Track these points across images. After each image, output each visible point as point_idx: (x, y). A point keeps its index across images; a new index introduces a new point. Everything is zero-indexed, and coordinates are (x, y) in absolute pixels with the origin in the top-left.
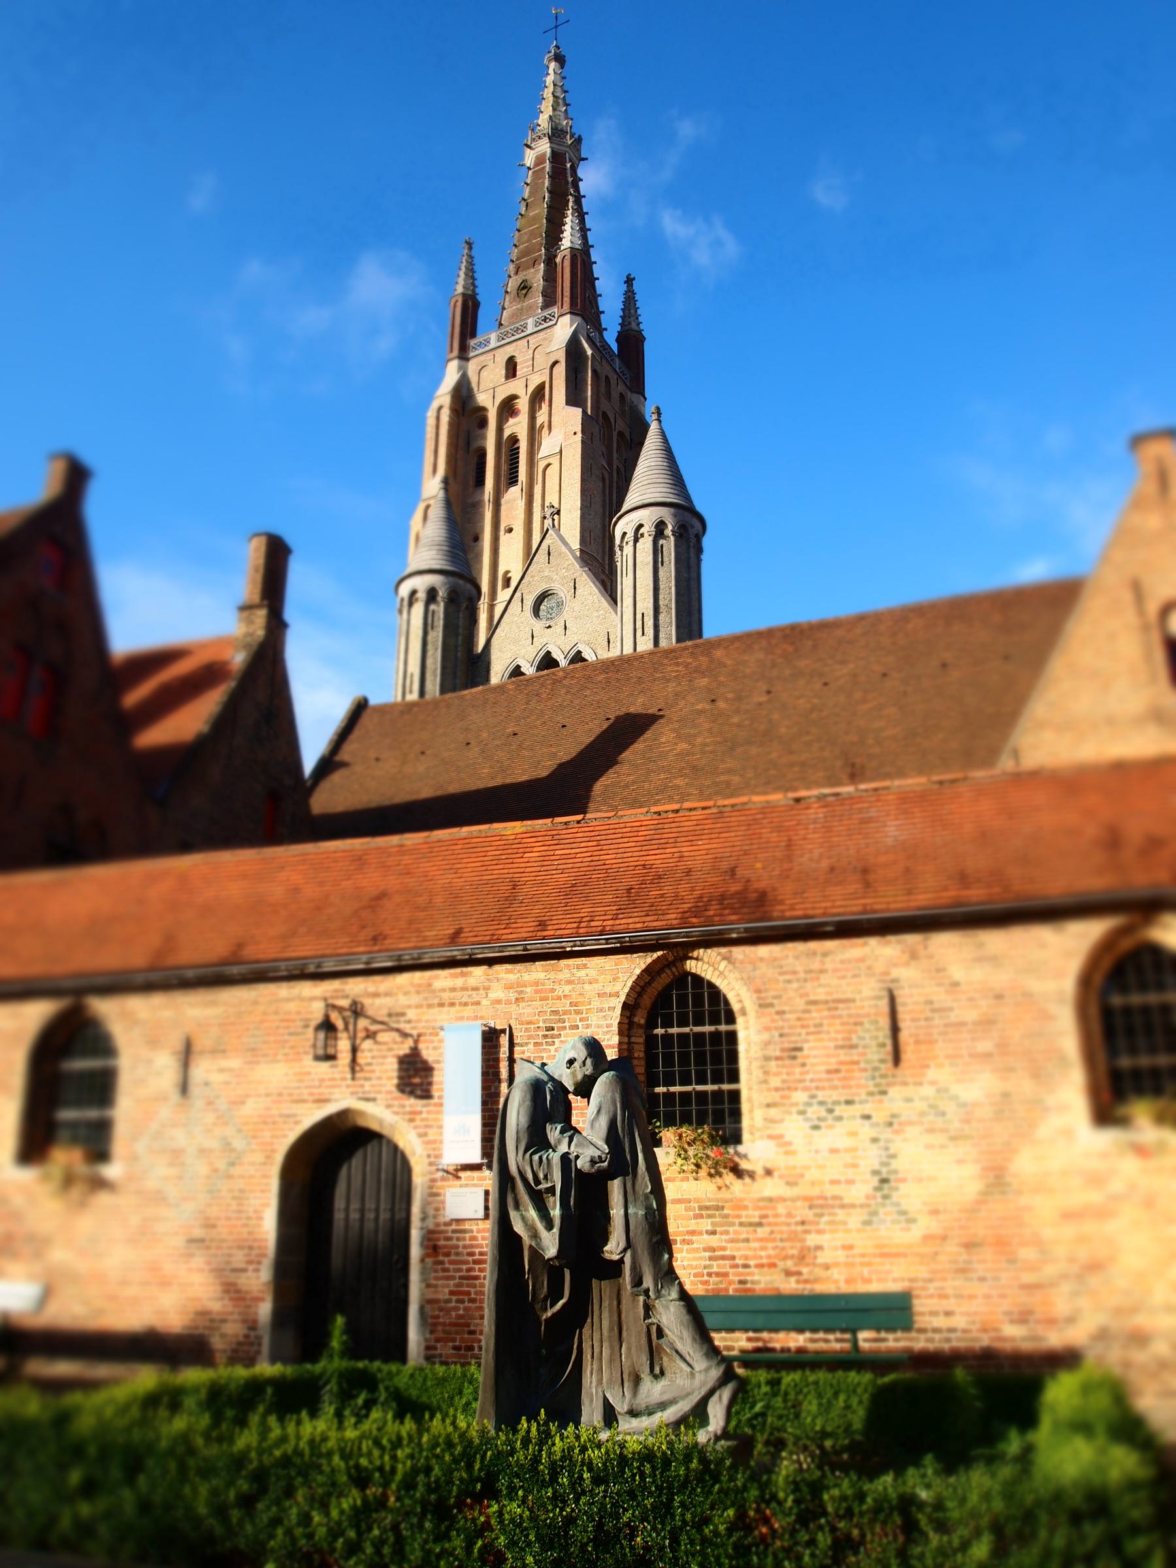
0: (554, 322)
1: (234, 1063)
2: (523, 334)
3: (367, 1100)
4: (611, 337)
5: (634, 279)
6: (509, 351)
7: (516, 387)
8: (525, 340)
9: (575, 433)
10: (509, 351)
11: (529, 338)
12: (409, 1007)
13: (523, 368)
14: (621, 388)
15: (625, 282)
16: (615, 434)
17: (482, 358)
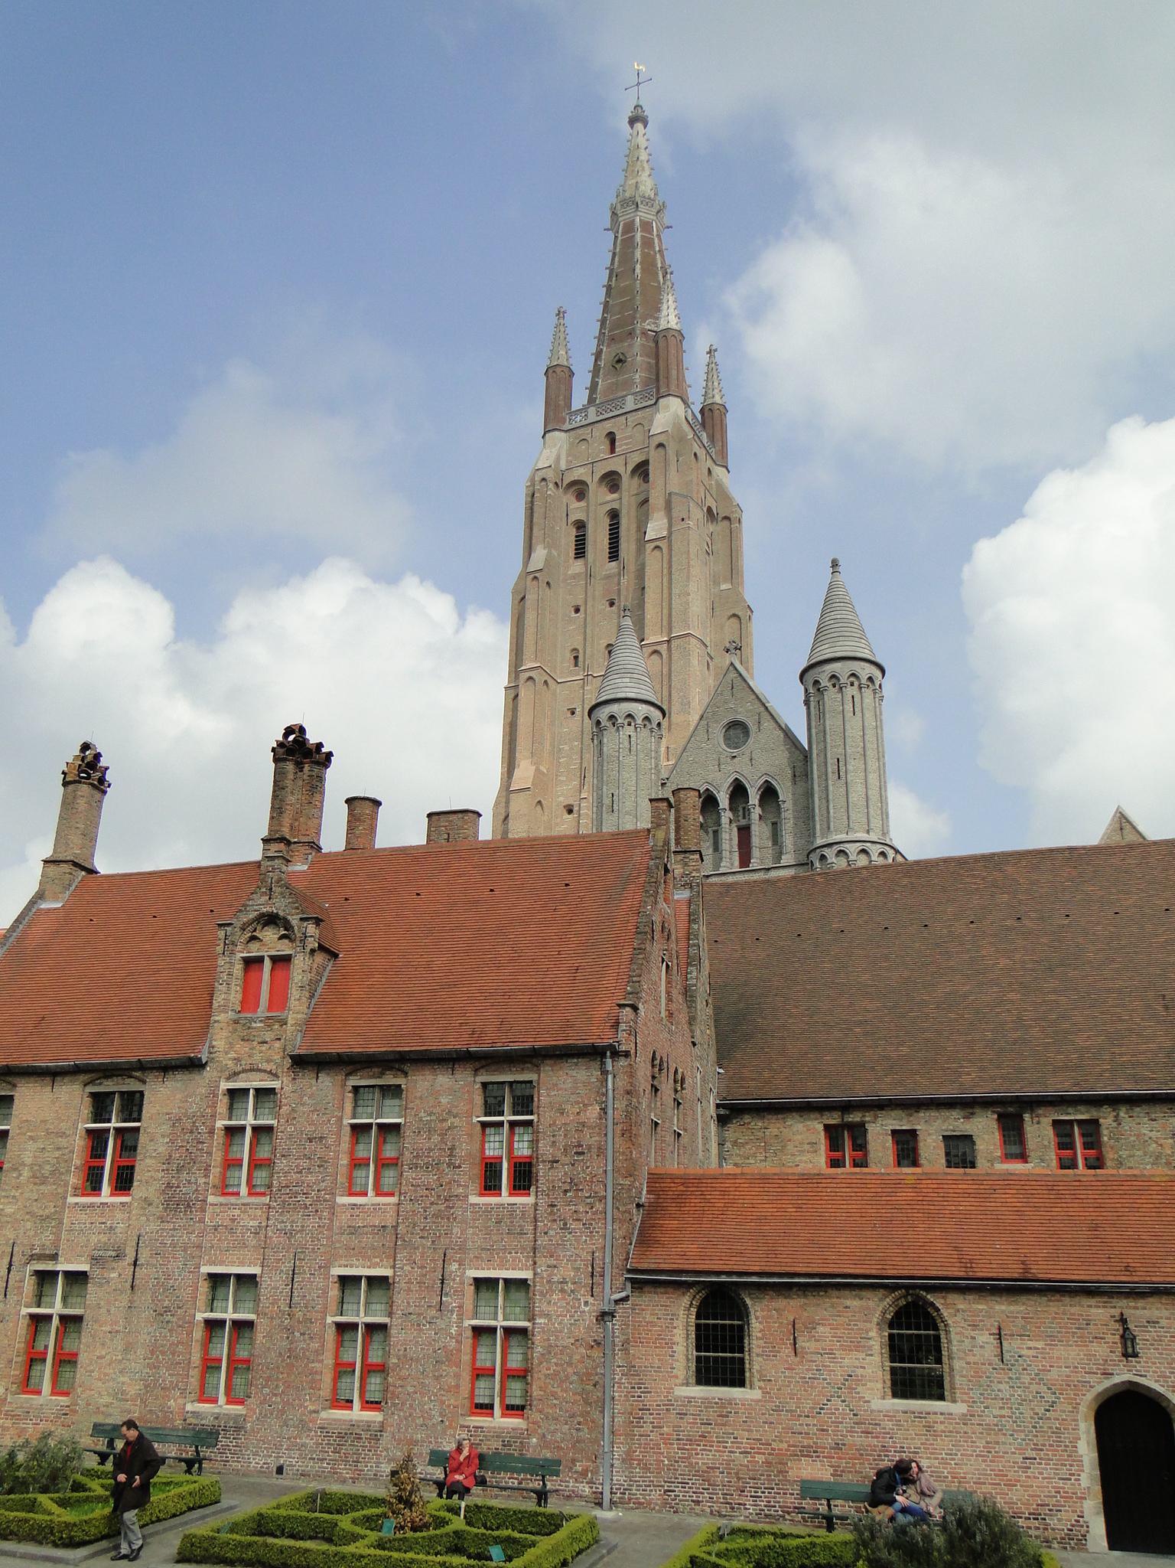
0: (653, 402)
1: (1040, 1345)
2: (624, 411)
3: (1141, 1376)
4: (697, 409)
5: (716, 350)
6: (608, 426)
7: (616, 465)
8: (624, 417)
9: (683, 520)
10: (608, 426)
11: (628, 415)
12: (1162, 1318)
13: (621, 445)
14: (709, 463)
15: (708, 353)
16: (705, 509)
17: (579, 431)
